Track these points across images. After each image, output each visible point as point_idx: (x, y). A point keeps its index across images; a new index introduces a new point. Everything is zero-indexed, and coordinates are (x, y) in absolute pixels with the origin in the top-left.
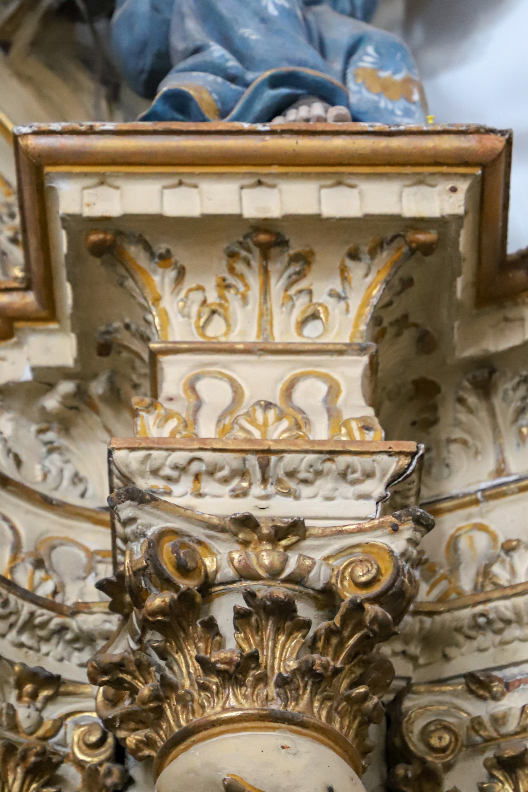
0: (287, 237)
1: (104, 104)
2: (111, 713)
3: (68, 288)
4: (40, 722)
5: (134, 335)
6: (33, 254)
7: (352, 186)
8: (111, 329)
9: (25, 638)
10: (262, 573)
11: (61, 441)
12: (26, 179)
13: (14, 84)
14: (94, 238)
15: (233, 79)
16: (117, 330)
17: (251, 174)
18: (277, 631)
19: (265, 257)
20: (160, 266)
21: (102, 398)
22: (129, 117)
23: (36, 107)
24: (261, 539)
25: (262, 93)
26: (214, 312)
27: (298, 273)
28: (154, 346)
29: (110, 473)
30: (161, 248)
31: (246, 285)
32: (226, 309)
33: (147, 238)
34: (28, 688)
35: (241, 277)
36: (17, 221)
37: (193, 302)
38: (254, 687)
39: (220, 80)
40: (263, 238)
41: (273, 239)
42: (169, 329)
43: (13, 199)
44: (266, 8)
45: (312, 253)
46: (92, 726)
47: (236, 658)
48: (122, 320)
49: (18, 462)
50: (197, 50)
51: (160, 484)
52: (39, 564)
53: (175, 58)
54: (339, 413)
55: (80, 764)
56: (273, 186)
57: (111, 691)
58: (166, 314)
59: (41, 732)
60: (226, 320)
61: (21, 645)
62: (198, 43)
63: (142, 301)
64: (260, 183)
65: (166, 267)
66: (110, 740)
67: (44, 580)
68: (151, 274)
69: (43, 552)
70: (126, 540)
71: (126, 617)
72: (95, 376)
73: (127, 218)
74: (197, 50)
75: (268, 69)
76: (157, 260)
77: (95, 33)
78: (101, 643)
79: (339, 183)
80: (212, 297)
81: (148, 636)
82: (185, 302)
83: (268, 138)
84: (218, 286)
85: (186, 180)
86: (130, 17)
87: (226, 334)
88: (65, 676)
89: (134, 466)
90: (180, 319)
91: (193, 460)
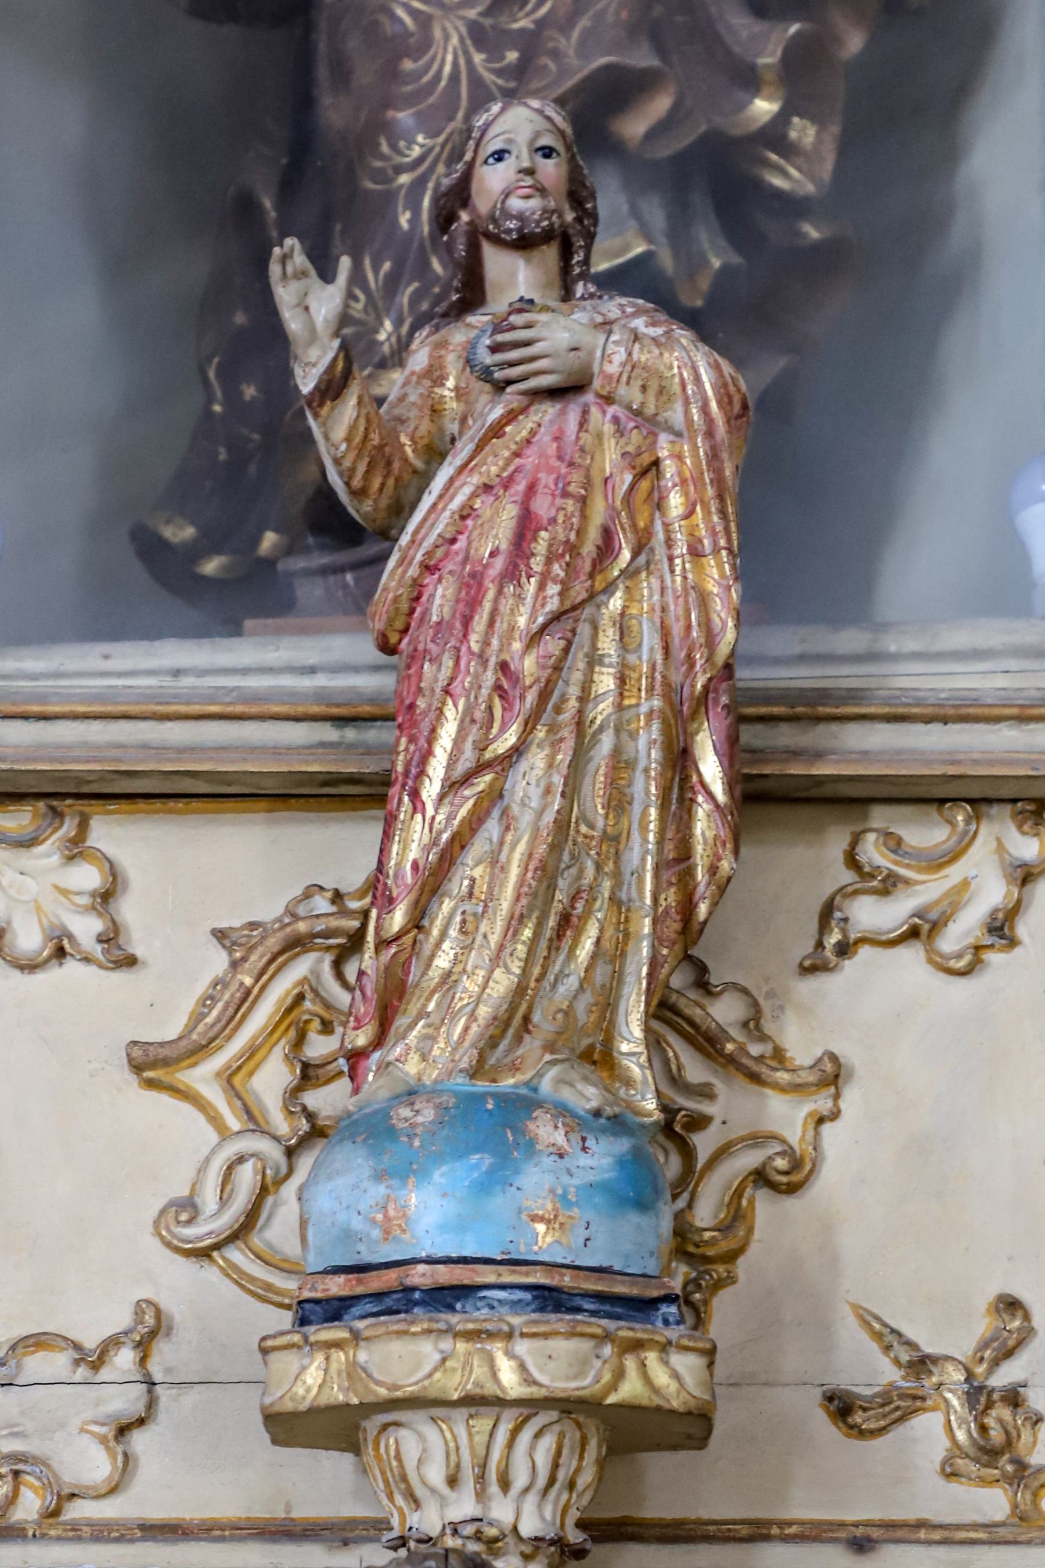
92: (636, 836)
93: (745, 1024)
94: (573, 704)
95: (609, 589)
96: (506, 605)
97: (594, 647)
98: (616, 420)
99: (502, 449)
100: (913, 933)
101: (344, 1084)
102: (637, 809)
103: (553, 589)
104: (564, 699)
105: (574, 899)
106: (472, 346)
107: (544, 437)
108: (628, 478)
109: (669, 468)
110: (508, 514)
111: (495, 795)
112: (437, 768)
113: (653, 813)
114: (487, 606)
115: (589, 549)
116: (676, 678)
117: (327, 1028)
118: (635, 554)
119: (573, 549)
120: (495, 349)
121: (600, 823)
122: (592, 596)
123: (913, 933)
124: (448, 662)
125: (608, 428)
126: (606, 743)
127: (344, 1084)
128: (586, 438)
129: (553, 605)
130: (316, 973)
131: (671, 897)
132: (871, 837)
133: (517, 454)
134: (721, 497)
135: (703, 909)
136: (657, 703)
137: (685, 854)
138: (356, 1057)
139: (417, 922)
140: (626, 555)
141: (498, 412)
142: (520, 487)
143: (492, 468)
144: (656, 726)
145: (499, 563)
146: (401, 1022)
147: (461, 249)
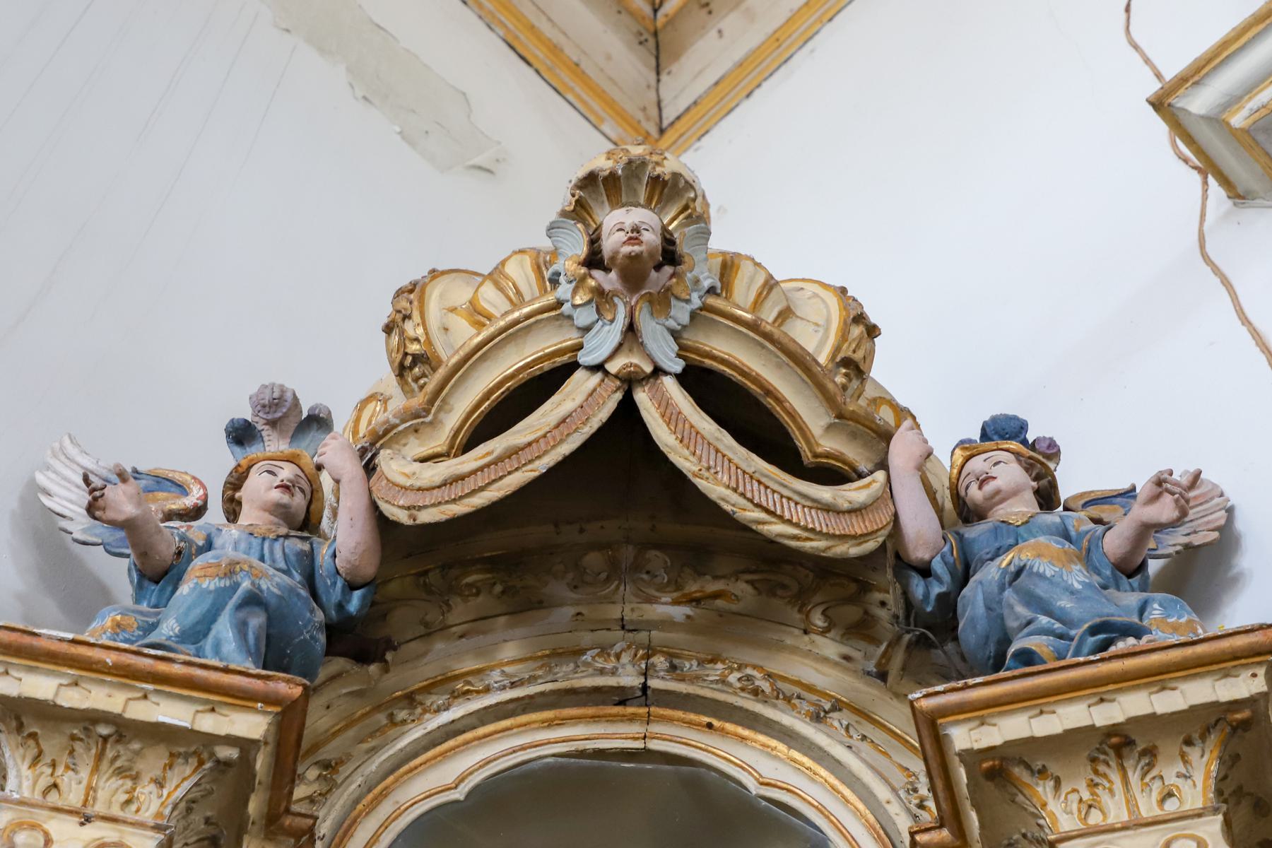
0: (1133, 737)
3: (974, 815)
5: (1031, 842)
7: (1174, 689)
8: (1012, 841)
15: (1061, 636)
16: (1017, 842)
17: (1094, 694)
19: (1120, 756)
20: (1041, 779)
25: (1086, 640)
26: (1090, 806)
27: (1148, 764)
30: (1038, 765)
31: (1110, 781)
32: (1099, 802)
33: (1026, 759)
35: (1105, 776)
37: (1072, 802)
39: (1051, 638)
40: (1114, 740)
41: (1123, 740)
42: (1059, 825)
44: (1072, 584)
45: (1155, 747)
48: (1020, 832)
50: (1029, 623)
56: (1113, 701)
58: (1054, 814)
60: (1101, 810)
62: (1029, 618)
63: (1033, 810)
64: (1102, 700)
65: (1046, 779)
68: (1035, 786)
74: (1029, 623)
75: (1086, 623)
76: (1037, 775)
79: (1163, 689)
80: (1086, 795)
82: (1066, 803)
83: (1100, 664)
84: (1088, 786)
85: (1045, 709)
86: (972, 620)
87: (1104, 821)
90: (1065, 816)
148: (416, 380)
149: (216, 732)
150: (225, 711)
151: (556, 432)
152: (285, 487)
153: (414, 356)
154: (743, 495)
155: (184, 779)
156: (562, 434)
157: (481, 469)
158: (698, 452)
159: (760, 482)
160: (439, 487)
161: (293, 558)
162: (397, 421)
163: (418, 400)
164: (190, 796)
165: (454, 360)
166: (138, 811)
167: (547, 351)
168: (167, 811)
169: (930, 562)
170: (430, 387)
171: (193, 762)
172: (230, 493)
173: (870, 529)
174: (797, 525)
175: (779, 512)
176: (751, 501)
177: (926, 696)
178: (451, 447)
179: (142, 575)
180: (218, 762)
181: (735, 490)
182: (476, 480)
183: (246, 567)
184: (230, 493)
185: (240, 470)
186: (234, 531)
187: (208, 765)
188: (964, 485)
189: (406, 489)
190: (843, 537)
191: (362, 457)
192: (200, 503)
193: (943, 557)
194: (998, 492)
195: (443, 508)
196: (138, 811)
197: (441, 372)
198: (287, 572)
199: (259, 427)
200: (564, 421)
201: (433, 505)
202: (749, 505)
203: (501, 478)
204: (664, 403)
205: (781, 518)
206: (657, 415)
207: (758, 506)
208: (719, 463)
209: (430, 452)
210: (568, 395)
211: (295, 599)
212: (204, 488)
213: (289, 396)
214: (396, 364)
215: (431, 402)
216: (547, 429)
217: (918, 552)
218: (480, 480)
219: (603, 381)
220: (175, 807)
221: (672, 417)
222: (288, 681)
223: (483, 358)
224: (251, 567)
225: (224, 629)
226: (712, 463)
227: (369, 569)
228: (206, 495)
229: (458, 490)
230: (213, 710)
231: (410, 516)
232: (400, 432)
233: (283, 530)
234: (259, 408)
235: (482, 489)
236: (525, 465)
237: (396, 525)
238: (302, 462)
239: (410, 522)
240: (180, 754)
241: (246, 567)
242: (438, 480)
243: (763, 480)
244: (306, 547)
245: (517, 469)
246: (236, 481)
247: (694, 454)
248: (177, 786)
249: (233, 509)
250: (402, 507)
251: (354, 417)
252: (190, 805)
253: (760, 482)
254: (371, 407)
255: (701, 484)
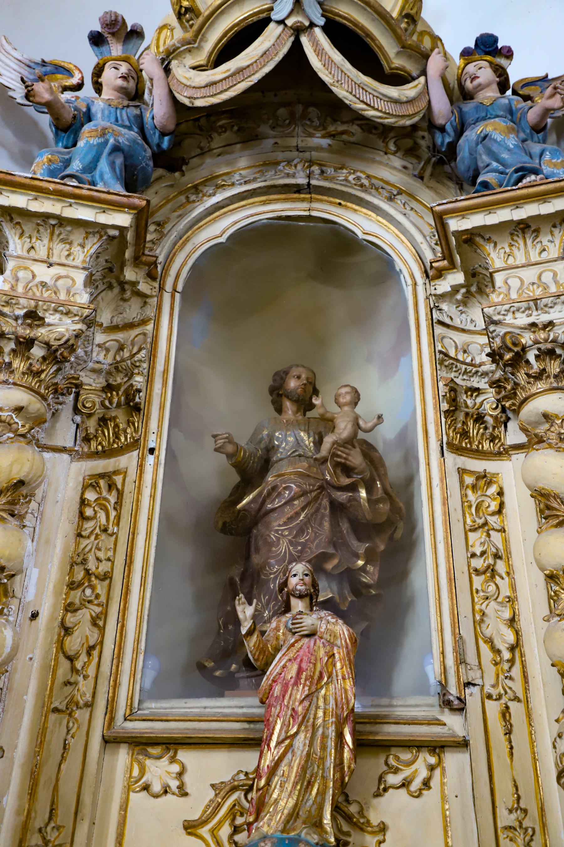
1: (458, 191)
2: (498, 397)
3: (458, 256)
4: (475, 404)
6: (444, 247)
9: (465, 377)
10: (542, 341)
11: (464, 309)
12: (437, 221)
13: (427, 190)
14: (464, 237)
18: (551, 360)
21: (475, 292)
22: (468, 193)
23: (435, 196)
24: (539, 329)
28: (490, 271)
29: (484, 316)
34: (469, 393)
36: (437, 237)
38: (546, 380)
43: (434, 230)
46: (493, 403)
47: (538, 371)
49: (452, 319)
51: (501, 317)
52: (465, 352)
53: (480, 170)
54: (558, 281)
55: (491, 416)
57: (497, 389)
59: (476, 407)
61: (464, 380)
66: (500, 406)
67: (467, 357)
69: (465, 347)
70: (493, 338)
71: (498, 364)
72: (472, 285)
73: (474, 228)
77: (451, 167)
78: (491, 375)
80: (508, 250)
81: (507, 369)
86: (463, 159)
87: (515, 262)
88: (481, 387)
89: (491, 312)
91: (511, 307)
92: (328, 757)
93: (359, 813)
94: (312, 720)
95: (322, 688)
96: (294, 692)
97: (317, 704)
98: (323, 643)
99: (294, 650)
100: (403, 785)
101: (245, 833)
102: (329, 750)
103: (307, 688)
104: (309, 718)
105: (311, 776)
106: (287, 622)
107: (305, 647)
108: (326, 658)
109: (337, 656)
110: (295, 667)
111: (290, 746)
112: (275, 738)
113: (333, 751)
114: (289, 692)
115: (316, 677)
116: (339, 712)
117: (242, 815)
118: (328, 679)
119: (312, 677)
120: (293, 624)
121: (319, 754)
122: (317, 690)
123: (403, 785)
124: (278, 708)
125: (321, 645)
126: (321, 731)
127: (245, 833)
128: (316, 648)
129: (306, 692)
130: (239, 798)
131: (338, 775)
132: (391, 756)
133: (298, 651)
134: (350, 664)
135: (347, 779)
136: (334, 719)
137: (342, 762)
138: (250, 825)
139: (268, 783)
140: (326, 679)
141: (293, 640)
142: (299, 660)
143: (291, 655)
144: (334, 726)
145: (293, 680)
146: (263, 814)
147: (285, 597)
148: (188, 21)
149: (107, 223)
150: (110, 212)
151: (261, 60)
152: (124, 78)
153: (186, 8)
154: (355, 96)
155: (94, 244)
156: (264, 61)
157: (225, 79)
158: (333, 72)
159: (363, 89)
160: (204, 87)
161: (132, 119)
162: (179, 45)
163: (189, 35)
164: (98, 251)
165: (207, 13)
166: (74, 259)
167: (255, 10)
168: (88, 260)
169: (445, 125)
170: (195, 28)
171: (97, 236)
172: (95, 79)
173: (416, 111)
174: (381, 111)
175: (372, 105)
176: (359, 99)
177: (438, 205)
178: (208, 61)
179: (57, 128)
180: (109, 236)
181: (351, 93)
182: (222, 85)
183: (110, 131)
184: (95, 79)
185: (100, 66)
186: (101, 103)
187: (105, 238)
188: (465, 77)
189: (187, 86)
190: (403, 116)
191: (162, 63)
192: (80, 81)
193: (451, 123)
194: (480, 85)
195: (207, 99)
196: (74, 259)
197: (201, 19)
198: (130, 128)
199: (106, 35)
200: (265, 53)
201: (202, 98)
202: (358, 101)
203: (235, 85)
204: (315, 44)
205: (373, 108)
206: (312, 51)
207: (362, 102)
208: (343, 78)
209: (198, 64)
210: (267, 37)
211: (136, 146)
212: (81, 72)
213: (120, 18)
214: (177, 12)
215: (196, 36)
216: (257, 58)
217: (440, 120)
218: (225, 85)
219: (284, 29)
220: (91, 257)
221: (320, 52)
222: (139, 198)
223: (222, 13)
224: (113, 130)
225: (103, 165)
226: (339, 78)
227: (171, 127)
228: (83, 77)
229: (213, 90)
230: (104, 212)
231: (190, 102)
232: (181, 51)
233: (126, 103)
234: (105, 25)
235: (226, 90)
236: (246, 78)
237: (183, 105)
238: (131, 62)
239: (190, 105)
240: (90, 233)
241: (110, 131)
242: (203, 84)
243: (365, 87)
244: (137, 112)
245: (243, 81)
246: (98, 71)
247: (331, 73)
248: (91, 248)
249: (98, 88)
250: (186, 97)
251: (155, 38)
252: (97, 255)
253: (363, 89)
254: (165, 31)
255: (334, 89)
